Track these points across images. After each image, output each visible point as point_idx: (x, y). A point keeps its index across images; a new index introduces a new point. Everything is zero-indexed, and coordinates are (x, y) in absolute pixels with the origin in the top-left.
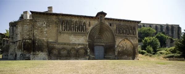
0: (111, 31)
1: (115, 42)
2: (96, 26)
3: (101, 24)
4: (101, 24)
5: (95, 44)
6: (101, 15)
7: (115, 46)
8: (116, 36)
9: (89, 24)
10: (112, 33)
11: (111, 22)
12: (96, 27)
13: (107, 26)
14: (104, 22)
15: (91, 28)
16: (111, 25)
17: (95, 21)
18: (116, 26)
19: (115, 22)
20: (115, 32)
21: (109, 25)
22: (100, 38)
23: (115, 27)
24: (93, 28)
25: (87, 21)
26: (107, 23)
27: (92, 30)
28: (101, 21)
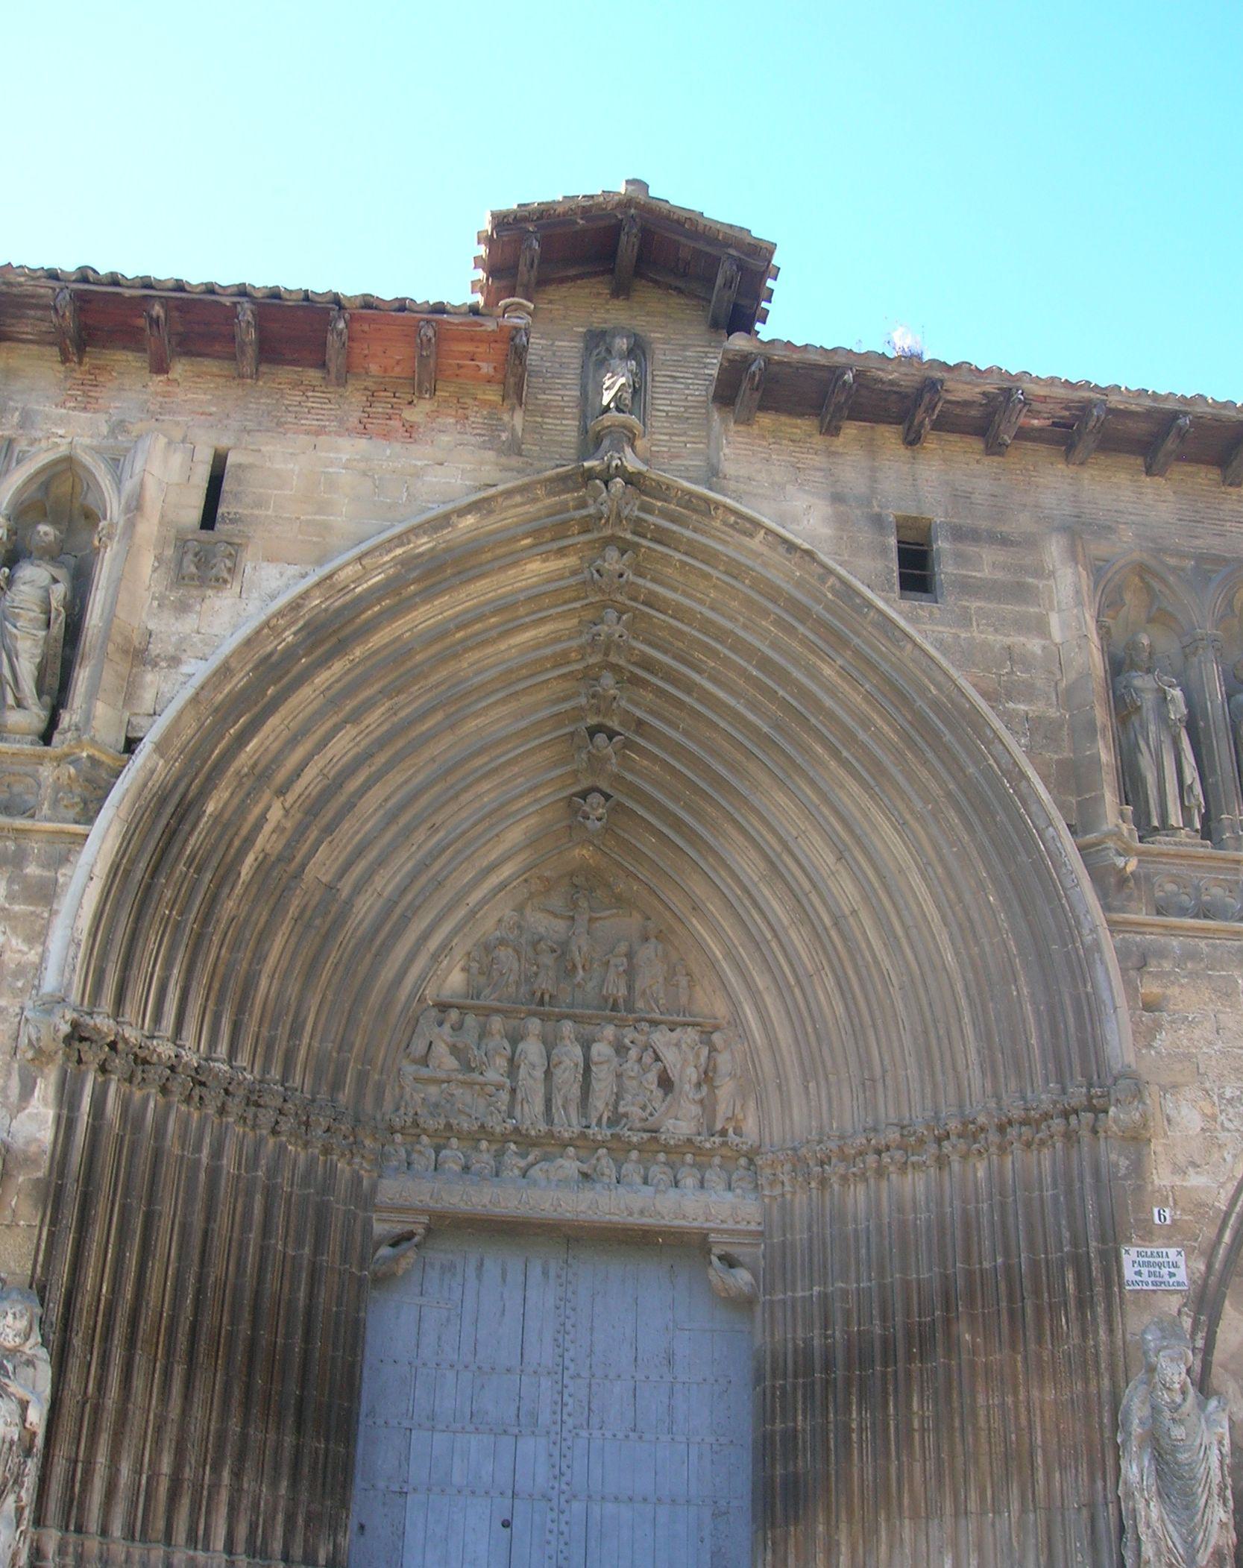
0: (935, 730)
1: (1085, 1099)
2: (435, 571)
3: (610, 520)
4: (610, 520)
5: (409, 1190)
6: (615, 315)
7: (1134, 1264)
8: (1113, 886)
9: (193, 514)
10: (989, 810)
11: (930, 480)
12: (424, 617)
13: (780, 572)
14: (713, 474)
15: (227, 622)
16: (916, 570)
17: (419, 455)
18: (1109, 603)
19: (1054, 485)
20: (1073, 779)
21: (872, 574)
22: (615, 1009)
23: (1067, 623)
24: (325, 631)
25: (149, 447)
26: (792, 498)
27: (263, 679)
28: (592, 441)
